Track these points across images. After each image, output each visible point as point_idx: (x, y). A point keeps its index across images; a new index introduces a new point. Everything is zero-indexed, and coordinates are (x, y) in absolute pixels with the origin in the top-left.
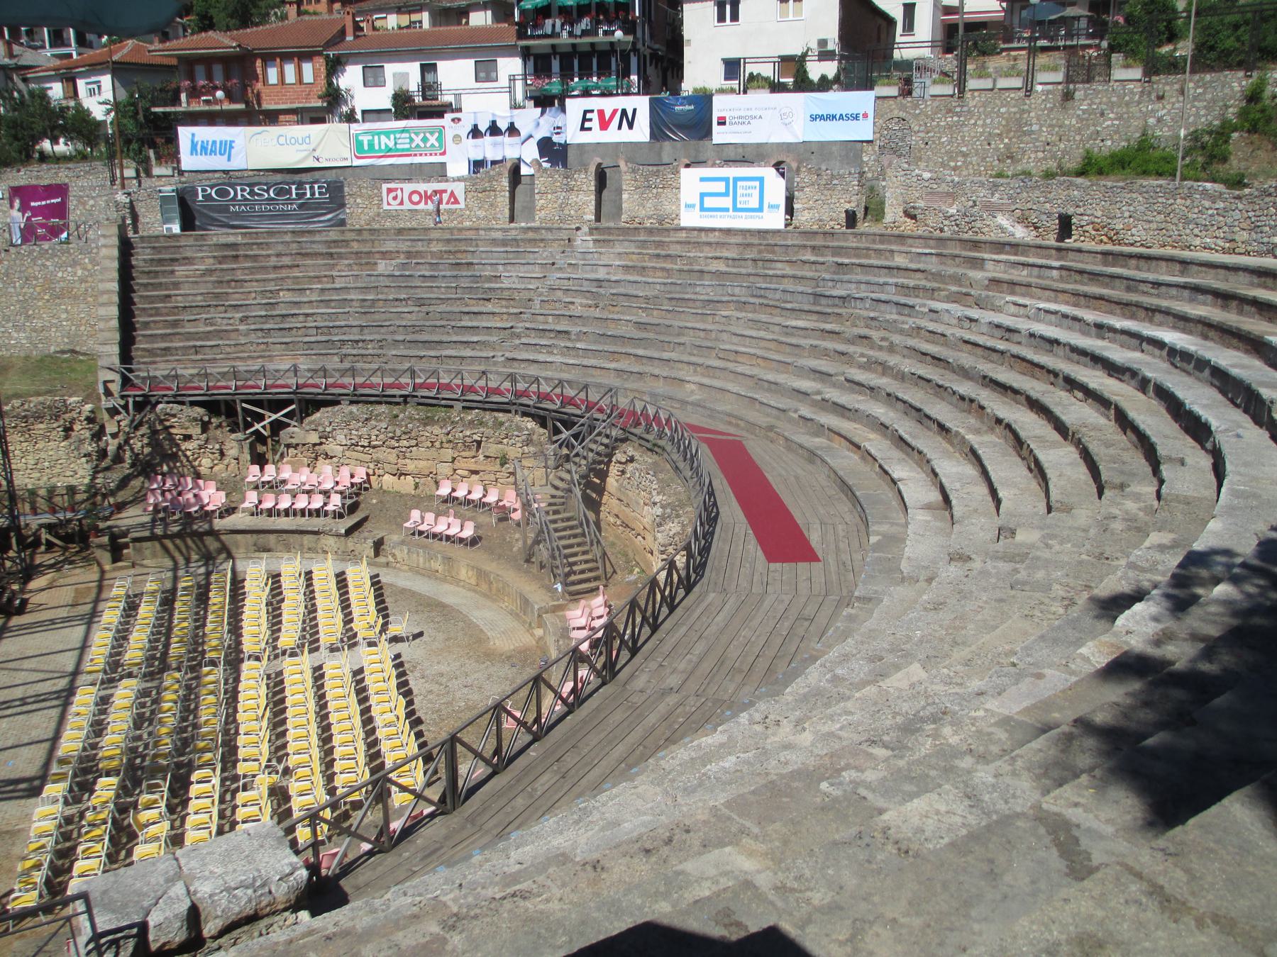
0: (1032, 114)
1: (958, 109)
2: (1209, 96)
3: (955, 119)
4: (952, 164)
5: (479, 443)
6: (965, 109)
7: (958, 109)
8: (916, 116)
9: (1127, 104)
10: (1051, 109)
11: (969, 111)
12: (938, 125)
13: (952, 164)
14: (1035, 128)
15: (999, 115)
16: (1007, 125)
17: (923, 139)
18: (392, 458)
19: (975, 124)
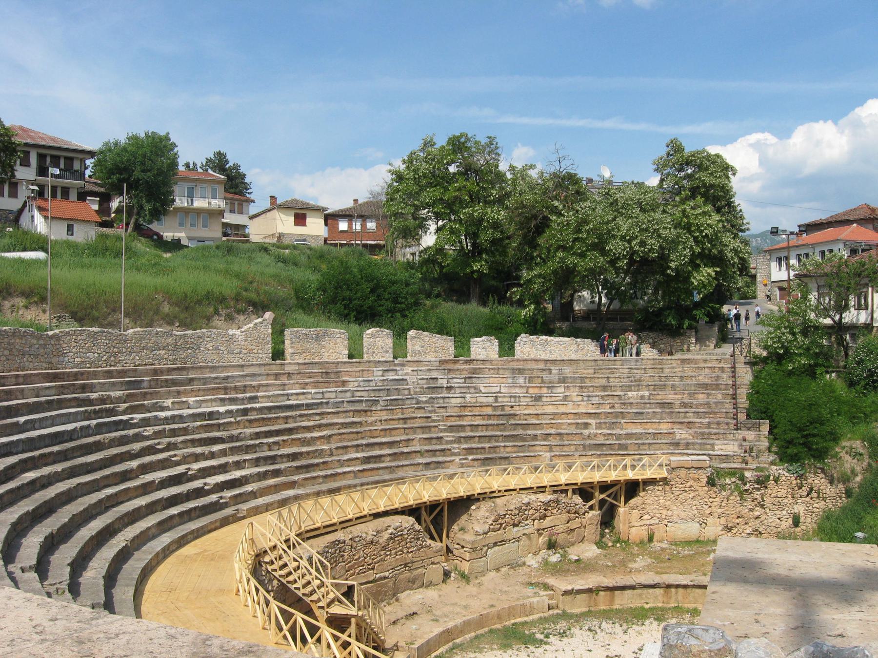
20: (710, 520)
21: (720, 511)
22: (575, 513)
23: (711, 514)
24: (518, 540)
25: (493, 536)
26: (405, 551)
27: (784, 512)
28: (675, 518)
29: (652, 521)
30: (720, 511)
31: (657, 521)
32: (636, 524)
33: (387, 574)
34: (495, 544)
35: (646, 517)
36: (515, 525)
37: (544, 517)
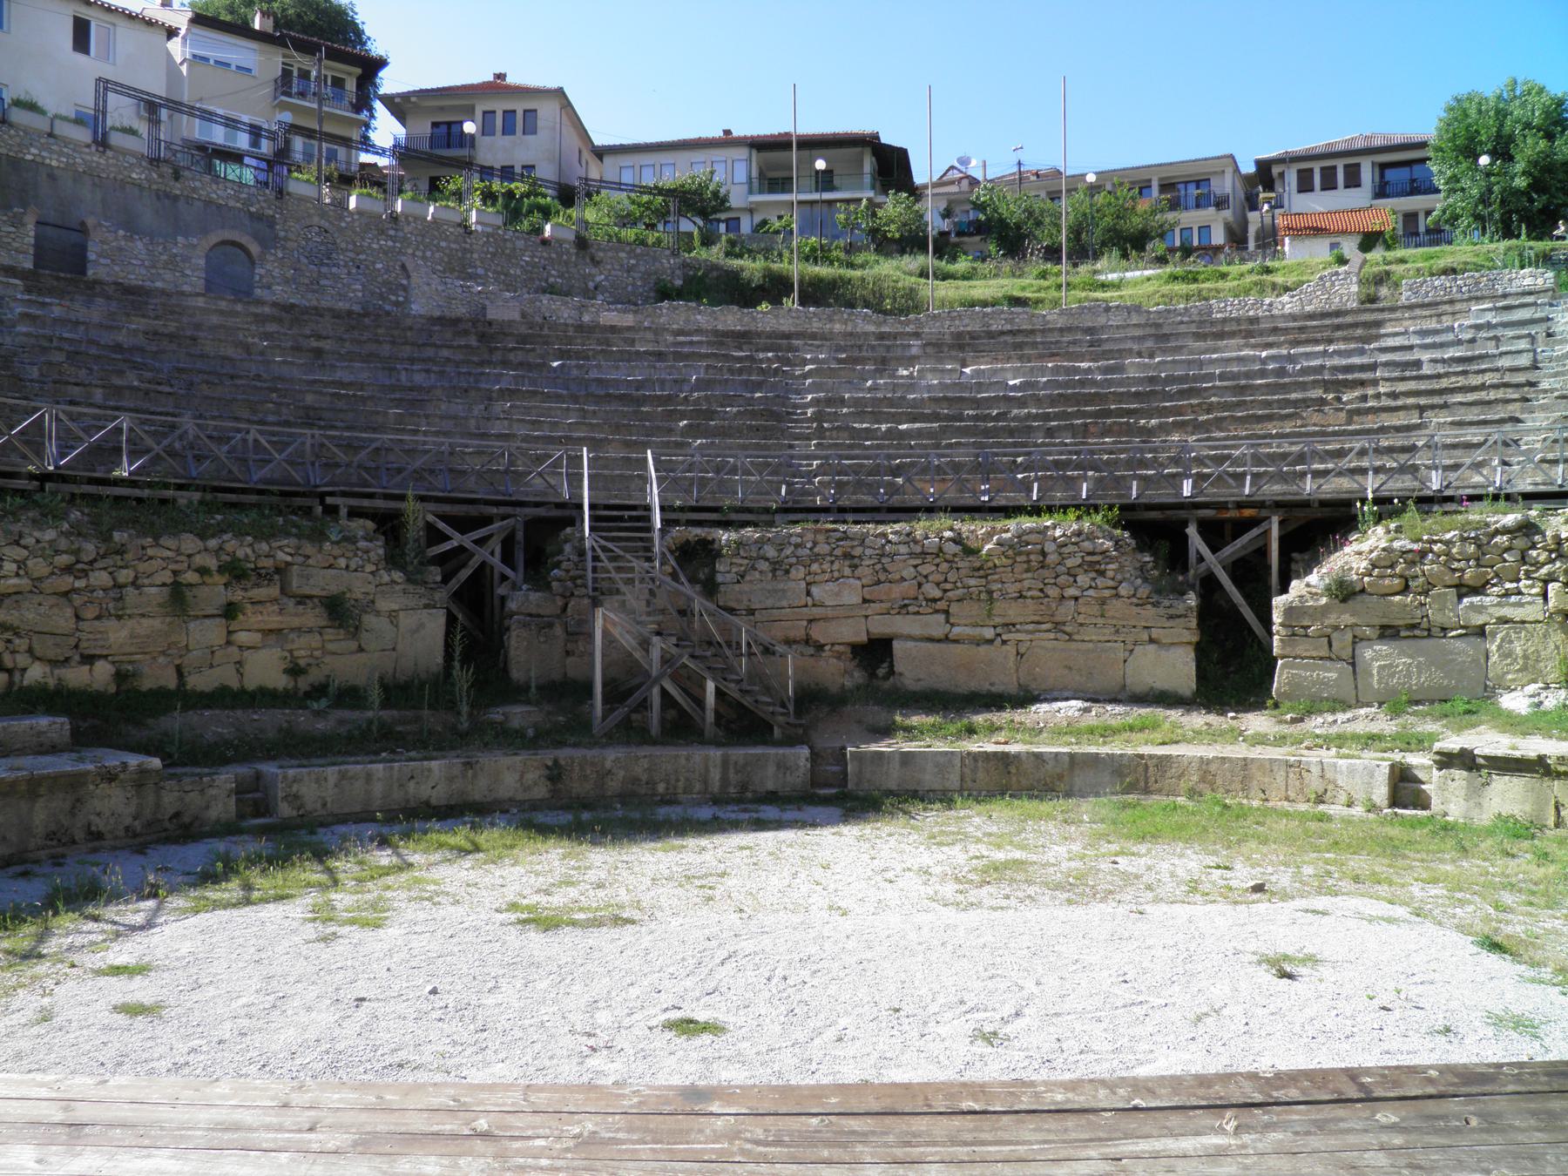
0: (475, 256)
1: (392, 232)
2: (642, 269)
3: (390, 243)
4: (393, 298)
6: (400, 234)
7: (392, 232)
8: (341, 230)
9: (566, 263)
10: (494, 255)
11: (405, 238)
12: (369, 247)
13: (393, 298)
14: (480, 271)
15: (439, 248)
16: (449, 263)
17: (353, 260)
19: (413, 255)
26: (1053, 592)
36: (1464, 589)
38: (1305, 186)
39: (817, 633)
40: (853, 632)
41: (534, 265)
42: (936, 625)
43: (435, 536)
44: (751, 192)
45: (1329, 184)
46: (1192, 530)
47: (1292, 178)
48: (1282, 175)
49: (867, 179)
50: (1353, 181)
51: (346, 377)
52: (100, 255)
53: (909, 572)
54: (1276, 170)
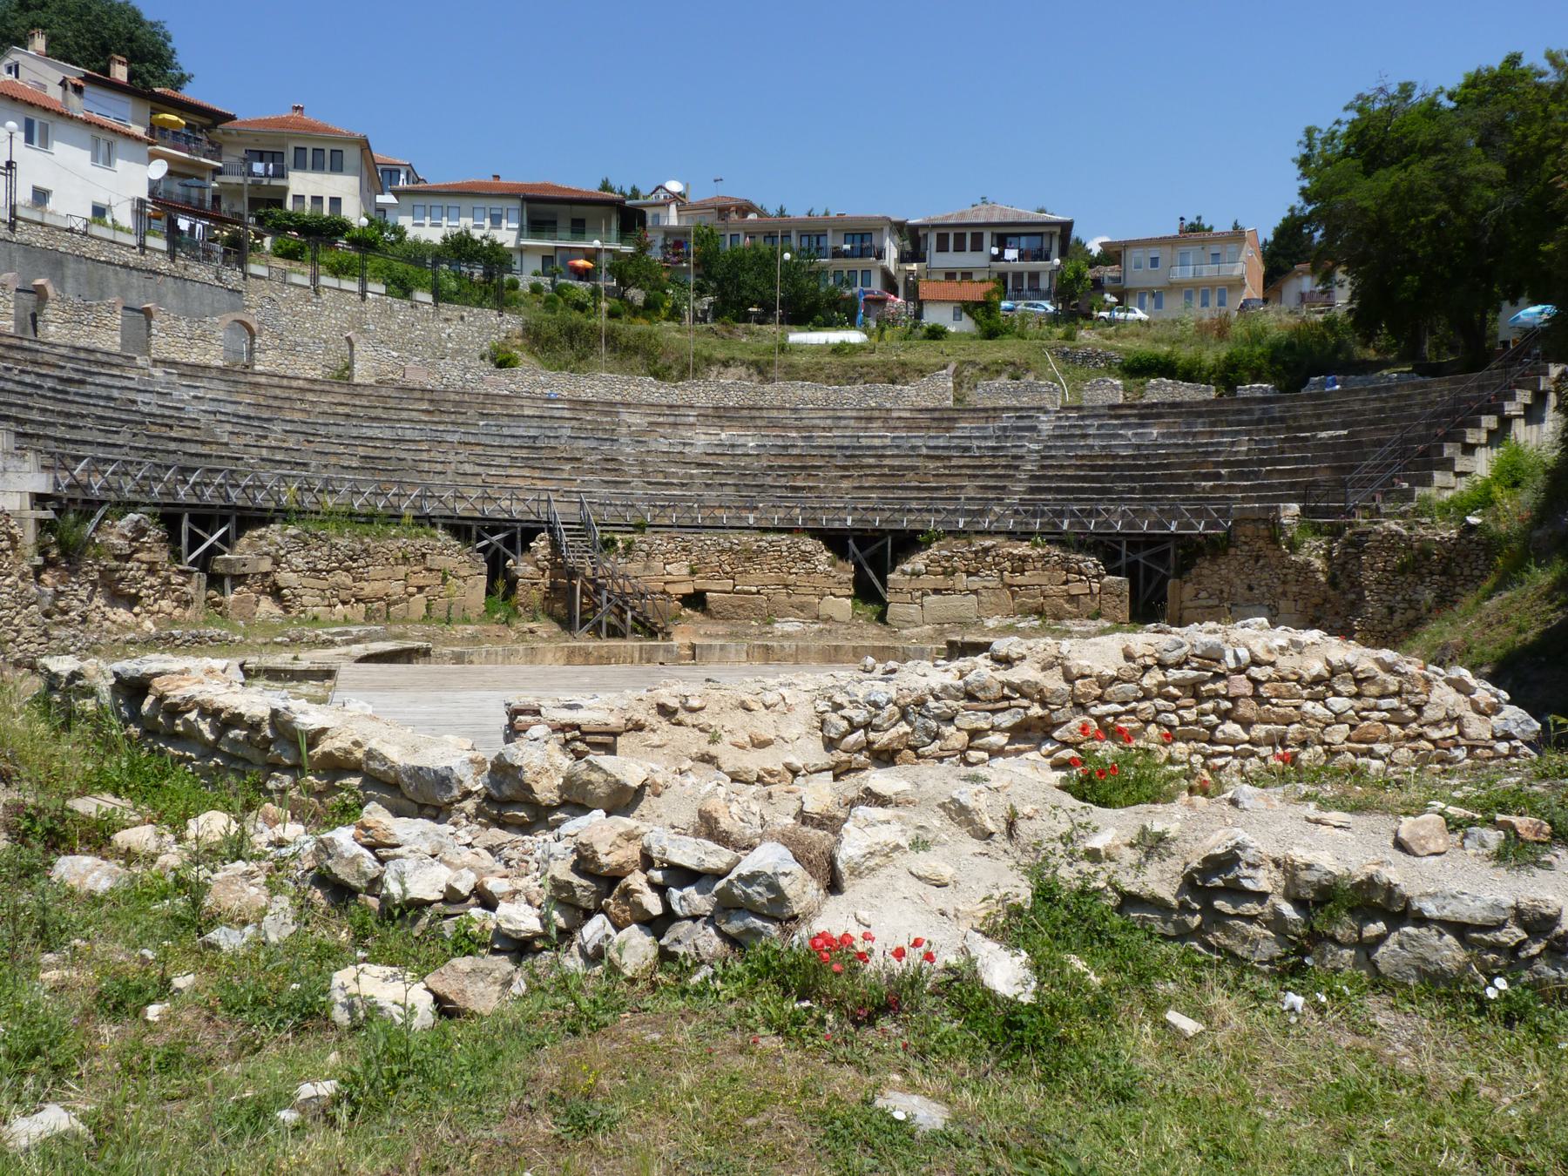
5: (424, 555)
18: (349, 581)
20: (1282, 604)
21: (1295, 589)
22: (1081, 573)
23: (1284, 594)
24: (975, 592)
25: (929, 582)
27: (1399, 598)
28: (1239, 600)
29: (1211, 603)
30: (1295, 589)
31: (1216, 602)
32: (1189, 604)
33: (754, 589)
34: (937, 591)
35: (1203, 594)
36: (969, 574)
37: (1022, 572)
38: (943, 247)
39: (669, 588)
40: (687, 589)
41: (406, 322)
42: (728, 584)
43: (480, 539)
44: (520, 236)
45: (959, 247)
46: (851, 542)
47: (933, 240)
48: (926, 236)
49: (614, 233)
50: (977, 246)
51: (370, 433)
52: (162, 330)
53: (714, 559)
54: (921, 233)
